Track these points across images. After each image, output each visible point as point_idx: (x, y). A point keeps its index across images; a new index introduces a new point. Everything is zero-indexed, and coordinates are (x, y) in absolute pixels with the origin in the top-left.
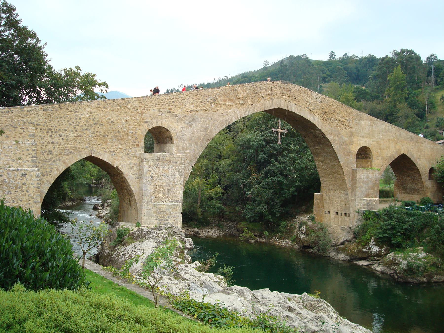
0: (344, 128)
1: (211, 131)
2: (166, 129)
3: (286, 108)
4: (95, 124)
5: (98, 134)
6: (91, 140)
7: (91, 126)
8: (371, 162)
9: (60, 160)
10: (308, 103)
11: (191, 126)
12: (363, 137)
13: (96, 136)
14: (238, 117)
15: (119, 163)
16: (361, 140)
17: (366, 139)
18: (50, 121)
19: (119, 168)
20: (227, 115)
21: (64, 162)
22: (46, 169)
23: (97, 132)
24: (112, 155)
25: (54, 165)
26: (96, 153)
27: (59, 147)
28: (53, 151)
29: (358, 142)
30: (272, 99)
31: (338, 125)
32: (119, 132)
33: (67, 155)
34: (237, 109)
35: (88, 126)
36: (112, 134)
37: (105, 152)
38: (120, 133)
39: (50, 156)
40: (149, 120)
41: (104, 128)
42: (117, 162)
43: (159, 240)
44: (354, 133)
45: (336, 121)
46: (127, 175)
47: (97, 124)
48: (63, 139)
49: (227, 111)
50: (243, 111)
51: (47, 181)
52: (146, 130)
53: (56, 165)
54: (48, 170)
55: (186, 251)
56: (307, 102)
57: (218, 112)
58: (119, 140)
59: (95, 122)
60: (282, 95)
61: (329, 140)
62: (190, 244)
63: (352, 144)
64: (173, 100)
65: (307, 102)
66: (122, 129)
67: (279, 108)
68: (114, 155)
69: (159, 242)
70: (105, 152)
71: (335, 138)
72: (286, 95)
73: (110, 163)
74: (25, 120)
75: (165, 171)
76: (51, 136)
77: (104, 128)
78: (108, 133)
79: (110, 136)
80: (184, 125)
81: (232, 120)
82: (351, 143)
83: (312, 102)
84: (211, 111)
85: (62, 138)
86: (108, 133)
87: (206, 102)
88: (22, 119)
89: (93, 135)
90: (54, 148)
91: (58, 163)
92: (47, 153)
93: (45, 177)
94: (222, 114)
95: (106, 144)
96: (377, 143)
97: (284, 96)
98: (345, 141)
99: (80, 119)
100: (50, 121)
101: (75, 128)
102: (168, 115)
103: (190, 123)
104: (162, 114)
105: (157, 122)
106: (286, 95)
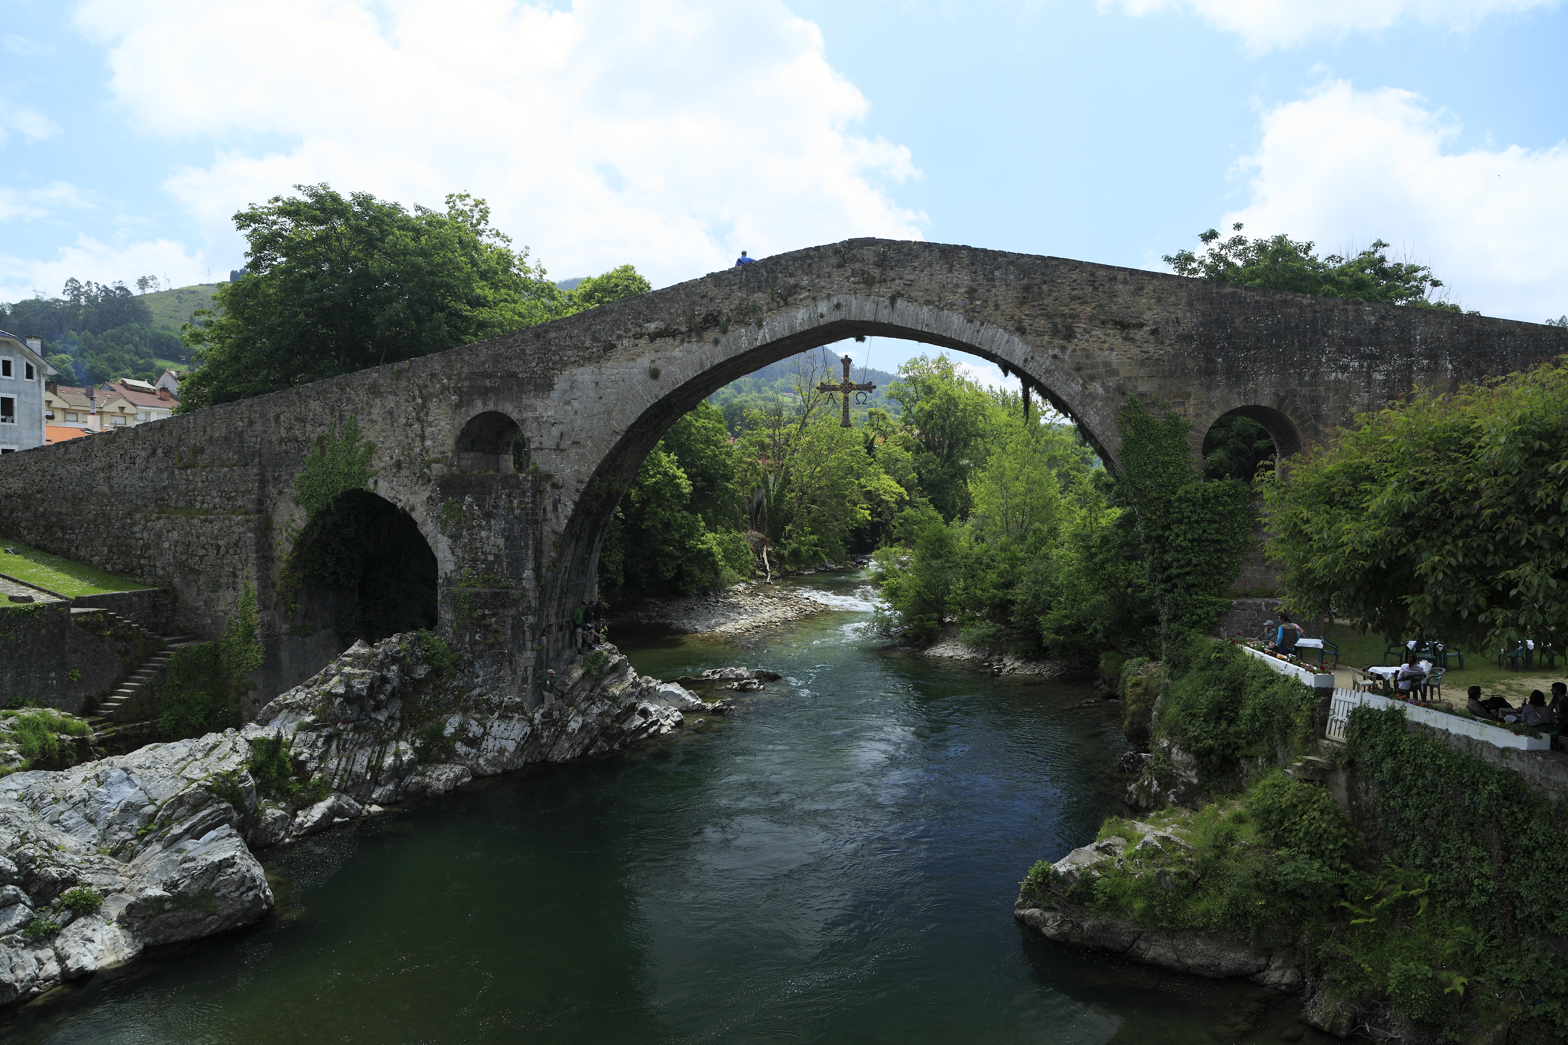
0: (1135, 351)
10: (963, 290)
11: (568, 403)
14: (702, 364)
19: (407, 509)
30: (814, 299)
31: (1106, 346)
36: (392, 438)
45: (1094, 333)
46: (424, 523)
56: (957, 286)
57: (639, 360)
61: (1064, 398)
62: (349, 686)
65: (957, 286)
67: (842, 321)
77: (377, 427)
79: (387, 445)
80: (548, 402)
96: (1328, 389)
103: (566, 397)
105: (484, 404)
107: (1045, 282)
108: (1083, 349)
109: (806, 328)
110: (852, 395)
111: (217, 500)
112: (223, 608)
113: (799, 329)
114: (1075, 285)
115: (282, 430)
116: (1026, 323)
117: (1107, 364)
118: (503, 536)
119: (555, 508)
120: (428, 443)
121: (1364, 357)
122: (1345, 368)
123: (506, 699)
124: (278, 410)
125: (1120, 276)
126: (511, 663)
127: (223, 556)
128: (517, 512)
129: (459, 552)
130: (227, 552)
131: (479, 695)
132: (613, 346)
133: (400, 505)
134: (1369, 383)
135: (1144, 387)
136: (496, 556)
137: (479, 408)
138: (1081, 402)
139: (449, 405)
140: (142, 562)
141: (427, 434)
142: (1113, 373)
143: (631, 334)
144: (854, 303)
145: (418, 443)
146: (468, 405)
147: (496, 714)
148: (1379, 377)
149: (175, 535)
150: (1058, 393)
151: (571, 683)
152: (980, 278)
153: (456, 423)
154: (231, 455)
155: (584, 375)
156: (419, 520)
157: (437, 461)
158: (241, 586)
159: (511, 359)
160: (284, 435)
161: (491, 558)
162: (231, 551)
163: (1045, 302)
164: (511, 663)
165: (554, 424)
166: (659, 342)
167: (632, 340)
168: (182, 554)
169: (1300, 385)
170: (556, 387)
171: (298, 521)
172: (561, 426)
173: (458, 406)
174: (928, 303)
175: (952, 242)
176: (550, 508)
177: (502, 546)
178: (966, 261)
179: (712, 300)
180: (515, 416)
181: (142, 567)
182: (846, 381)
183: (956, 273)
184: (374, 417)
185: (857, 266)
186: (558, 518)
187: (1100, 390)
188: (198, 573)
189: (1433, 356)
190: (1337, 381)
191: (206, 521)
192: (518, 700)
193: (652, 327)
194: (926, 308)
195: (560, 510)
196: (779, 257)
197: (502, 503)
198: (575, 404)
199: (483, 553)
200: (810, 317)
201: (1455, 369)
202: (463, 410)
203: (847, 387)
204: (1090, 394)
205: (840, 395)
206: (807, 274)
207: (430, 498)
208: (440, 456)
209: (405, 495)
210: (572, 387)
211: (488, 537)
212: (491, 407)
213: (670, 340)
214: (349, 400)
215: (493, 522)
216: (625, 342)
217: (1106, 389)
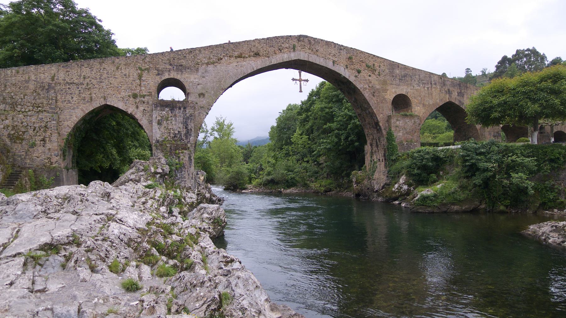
0: (375, 77)
1: (225, 81)
2: (178, 80)
3: (306, 59)
4: (108, 77)
5: (112, 86)
6: (106, 91)
7: (105, 79)
8: (412, 109)
9: (78, 108)
10: (332, 55)
11: (204, 77)
12: (399, 85)
13: (110, 88)
14: (253, 69)
15: (133, 109)
16: (397, 88)
17: (402, 87)
18: (68, 75)
19: (133, 114)
20: (241, 66)
21: (82, 110)
22: (66, 116)
23: (111, 84)
24: (126, 103)
25: (73, 113)
26: (111, 102)
27: (76, 97)
28: (71, 100)
29: (394, 90)
32: (132, 84)
33: (84, 104)
34: (253, 62)
35: (103, 79)
36: (126, 86)
37: (119, 100)
38: (133, 84)
39: (69, 105)
40: (160, 72)
41: (118, 80)
42: (130, 109)
43: (139, 168)
44: (388, 82)
45: (365, 71)
46: (141, 120)
47: (111, 77)
48: (80, 90)
49: (241, 63)
50: (259, 63)
51: (68, 126)
52: (158, 82)
53: (75, 112)
54: (68, 117)
55: (158, 176)
56: (330, 53)
57: (231, 65)
58: (132, 90)
59: (108, 76)
60: (302, 48)
61: (359, 88)
62: (163, 170)
63: (387, 92)
64: (185, 55)
66: (134, 81)
67: (299, 59)
68: (127, 103)
69: (139, 169)
70: (119, 100)
71: (365, 87)
72: (306, 48)
73: (124, 110)
74: (46, 75)
75: (175, 115)
76: (69, 88)
77: (118, 80)
78: (121, 84)
80: (196, 76)
81: (247, 70)
82: (385, 91)
83: (337, 54)
84: (225, 64)
85: (79, 89)
86: (121, 84)
87: (219, 56)
88: (43, 75)
89: (108, 87)
90: (72, 98)
91: (77, 111)
92: (66, 102)
93: (66, 122)
94: (236, 66)
95: (120, 94)
96: (416, 91)
97: (303, 48)
98: (378, 89)
99: (95, 74)
100: (68, 75)
101: (90, 81)
102: (180, 68)
104: (173, 67)
105: (169, 75)
106: (306, 48)
107: (353, 55)
108: (363, 75)
109: (287, 60)
110: (302, 82)
112: (37, 155)
113: (285, 60)
114: (361, 57)
116: (348, 66)
117: (369, 80)
118: (182, 123)
119: (199, 115)
120: (143, 88)
121: (423, 83)
122: (419, 86)
123: (186, 185)
125: (371, 56)
126: (188, 171)
128: (187, 115)
129: (162, 129)
131: (179, 183)
132: (221, 59)
133: (129, 112)
134: (425, 90)
135: (378, 87)
136: (179, 132)
137: (166, 76)
138: (363, 90)
139: (153, 75)
141: (142, 85)
142: (370, 82)
143: (228, 55)
144: (302, 54)
145: (138, 88)
146: (161, 75)
147: (185, 190)
148: (426, 89)
150: (358, 87)
151: (201, 181)
152: (337, 52)
153: (156, 81)
155: (211, 68)
156: (139, 119)
157: (148, 96)
159: (180, 59)
160: (69, 81)
161: (177, 132)
163: (353, 61)
164: (188, 171)
165: (198, 84)
166: (239, 59)
167: (229, 58)
169: (411, 89)
170: (199, 71)
172: (201, 85)
173: (158, 74)
174: (323, 57)
175: (329, 40)
176: (197, 115)
177: (182, 128)
178: (333, 46)
179: (257, 47)
180: (182, 80)
182: (300, 78)
183: (330, 50)
184: (116, 76)
185: (303, 43)
186: (201, 118)
187: (368, 87)
188: (22, 140)
189: (435, 84)
190: (418, 89)
192: (190, 185)
193: (236, 54)
194: (322, 59)
195: (201, 116)
196: (279, 37)
197: (181, 111)
198: (207, 77)
199: (172, 130)
200: (289, 58)
201: (440, 88)
202: (159, 77)
203: (300, 80)
204: (365, 88)
205: (298, 82)
206: (287, 44)
207: (144, 109)
208: (148, 94)
209: (132, 108)
210: (205, 72)
211: (175, 125)
212: (172, 76)
213: (242, 59)
214: (104, 68)
215: (177, 119)
216: (226, 58)
217: (369, 87)
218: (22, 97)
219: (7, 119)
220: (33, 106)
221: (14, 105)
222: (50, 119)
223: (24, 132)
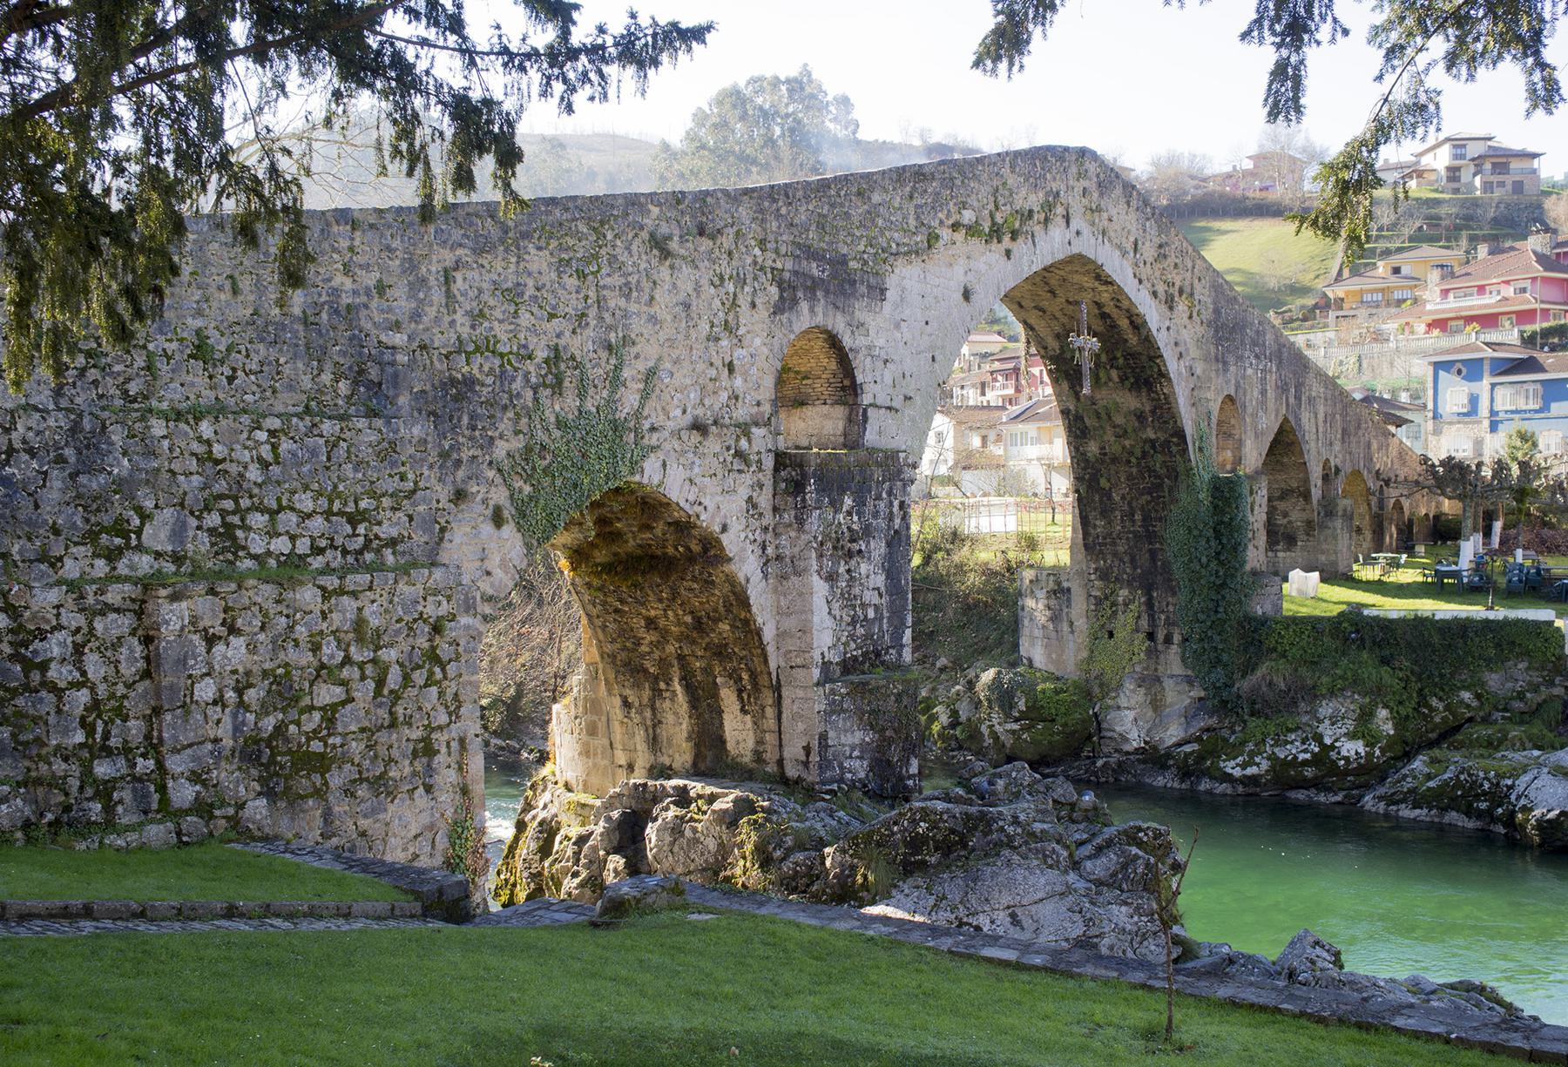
111: (317, 524)
115: (459, 317)
124: (448, 257)
127: (396, 696)
130: (406, 678)
140: (102, 769)
149: (233, 653)
154: (326, 378)
158: (447, 777)
160: (465, 331)
162: (419, 677)
168: (265, 710)
171: (498, 573)
181: (105, 791)
188: (321, 764)
191: (341, 592)
214: (613, 259)
218: (266, 451)
219: (233, 630)
220: (328, 514)
221: (224, 513)
222: (449, 598)
223: (330, 713)
